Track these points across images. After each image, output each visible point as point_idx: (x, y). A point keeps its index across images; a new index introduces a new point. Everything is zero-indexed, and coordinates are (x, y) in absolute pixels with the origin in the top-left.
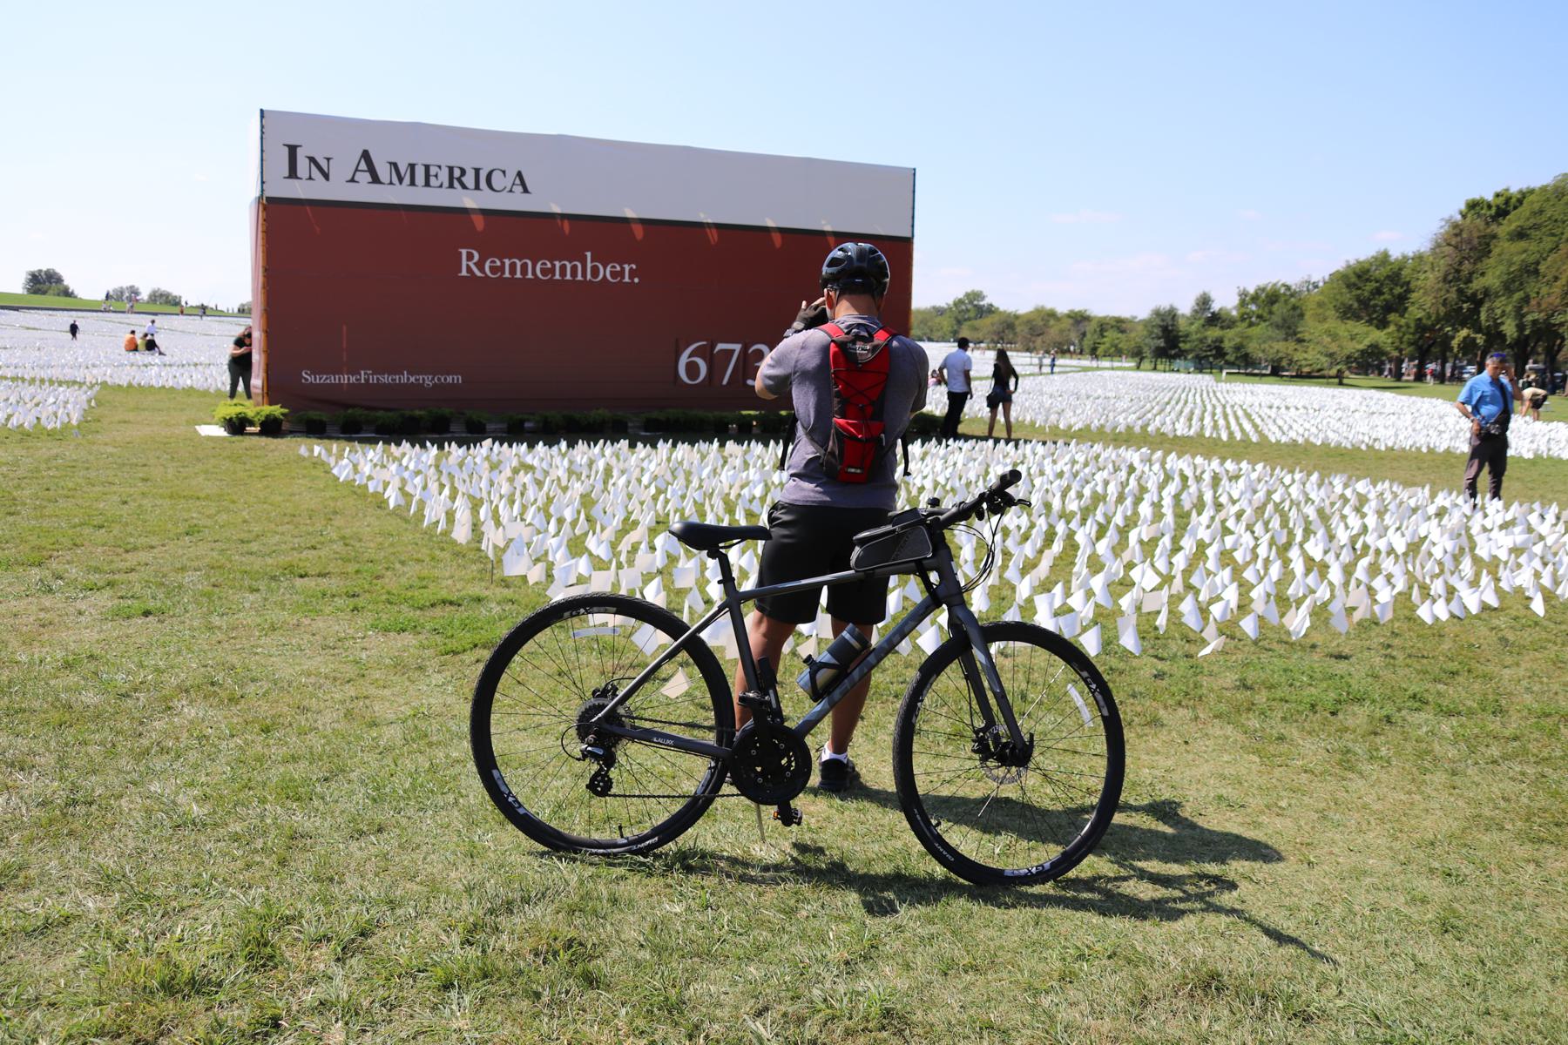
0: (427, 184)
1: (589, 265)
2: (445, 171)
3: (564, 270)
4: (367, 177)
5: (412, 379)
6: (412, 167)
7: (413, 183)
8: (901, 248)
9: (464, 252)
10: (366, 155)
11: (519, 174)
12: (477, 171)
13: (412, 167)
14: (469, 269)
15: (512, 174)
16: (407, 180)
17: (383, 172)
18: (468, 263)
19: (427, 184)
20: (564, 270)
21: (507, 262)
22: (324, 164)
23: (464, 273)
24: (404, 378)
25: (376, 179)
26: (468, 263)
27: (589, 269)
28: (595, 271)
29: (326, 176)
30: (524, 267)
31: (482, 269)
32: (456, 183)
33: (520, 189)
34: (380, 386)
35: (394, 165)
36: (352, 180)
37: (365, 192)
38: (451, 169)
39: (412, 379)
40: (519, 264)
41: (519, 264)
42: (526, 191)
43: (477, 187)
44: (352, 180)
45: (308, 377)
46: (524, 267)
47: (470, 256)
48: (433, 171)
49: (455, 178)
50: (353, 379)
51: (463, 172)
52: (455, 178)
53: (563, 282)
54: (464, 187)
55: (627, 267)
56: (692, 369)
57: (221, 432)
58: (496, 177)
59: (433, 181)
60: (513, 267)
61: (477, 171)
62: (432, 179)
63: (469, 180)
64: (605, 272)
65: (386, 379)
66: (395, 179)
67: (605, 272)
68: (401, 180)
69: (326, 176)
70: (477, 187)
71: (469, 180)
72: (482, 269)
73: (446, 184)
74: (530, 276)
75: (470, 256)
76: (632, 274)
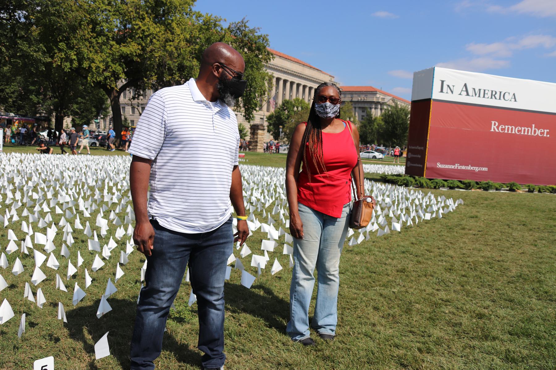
0: (484, 97)
1: (533, 129)
2: (490, 92)
4: (465, 93)
5: (472, 168)
6: (480, 90)
7: (479, 96)
9: (493, 122)
10: (465, 85)
11: (514, 94)
12: (501, 92)
13: (480, 90)
14: (494, 129)
15: (512, 94)
16: (478, 95)
19: (484, 97)
20: (526, 131)
21: (507, 127)
22: (452, 88)
23: (492, 130)
24: (469, 168)
25: (468, 94)
26: (494, 127)
27: (533, 131)
29: (452, 92)
30: (512, 129)
31: (498, 129)
32: (493, 97)
33: (514, 100)
34: (461, 170)
35: (474, 89)
36: (460, 94)
37: (464, 99)
38: (492, 91)
39: (472, 168)
40: (510, 128)
41: (510, 128)
42: (515, 101)
43: (500, 99)
44: (460, 94)
45: (439, 166)
46: (512, 129)
47: (495, 124)
48: (486, 92)
50: (453, 167)
51: (496, 93)
52: (493, 95)
53: (524, 135)
54: (496, 98)
55: (546, 131)
58: (506, 95)
59: (486, 96)
60: (508, 128)
61: (501, 92)
62: (486, 95)
63: (497, 96)
64: (538, 132)
65: (463, 167)
66: (474, 95)
67: (538, 132)
68: (476, 95)
69: (452, 92)
70: (500, 99)
71: (497, 96)
72: (498, 129)
73: (490, 97)
74: (513, 132)
75: (495, 124)
76: (547, 133)
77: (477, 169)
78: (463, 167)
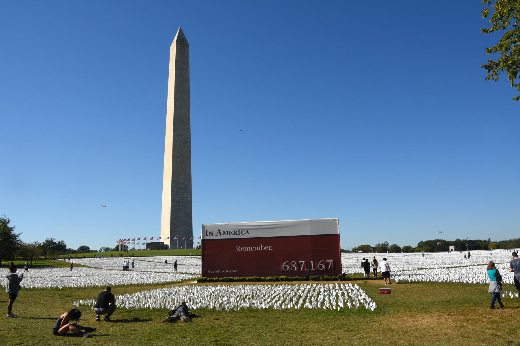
3: (257, 249)
8: (336, 237)
10: (219, 230)
15: (246, 231)
17: (222, 233)
18: (238, 249)
20: (257, 249)
28: (263, 248)
37: (219, 237)
49: (235, 233)
52: (235, 233)
53: (256, 251)
56: (285, 268)
57: (196, 282)
64: (265, 248)
65: (223, 272)
67: (265, 248)
76: (271, 248)
77: (231, 272)
78: (223, 272)
